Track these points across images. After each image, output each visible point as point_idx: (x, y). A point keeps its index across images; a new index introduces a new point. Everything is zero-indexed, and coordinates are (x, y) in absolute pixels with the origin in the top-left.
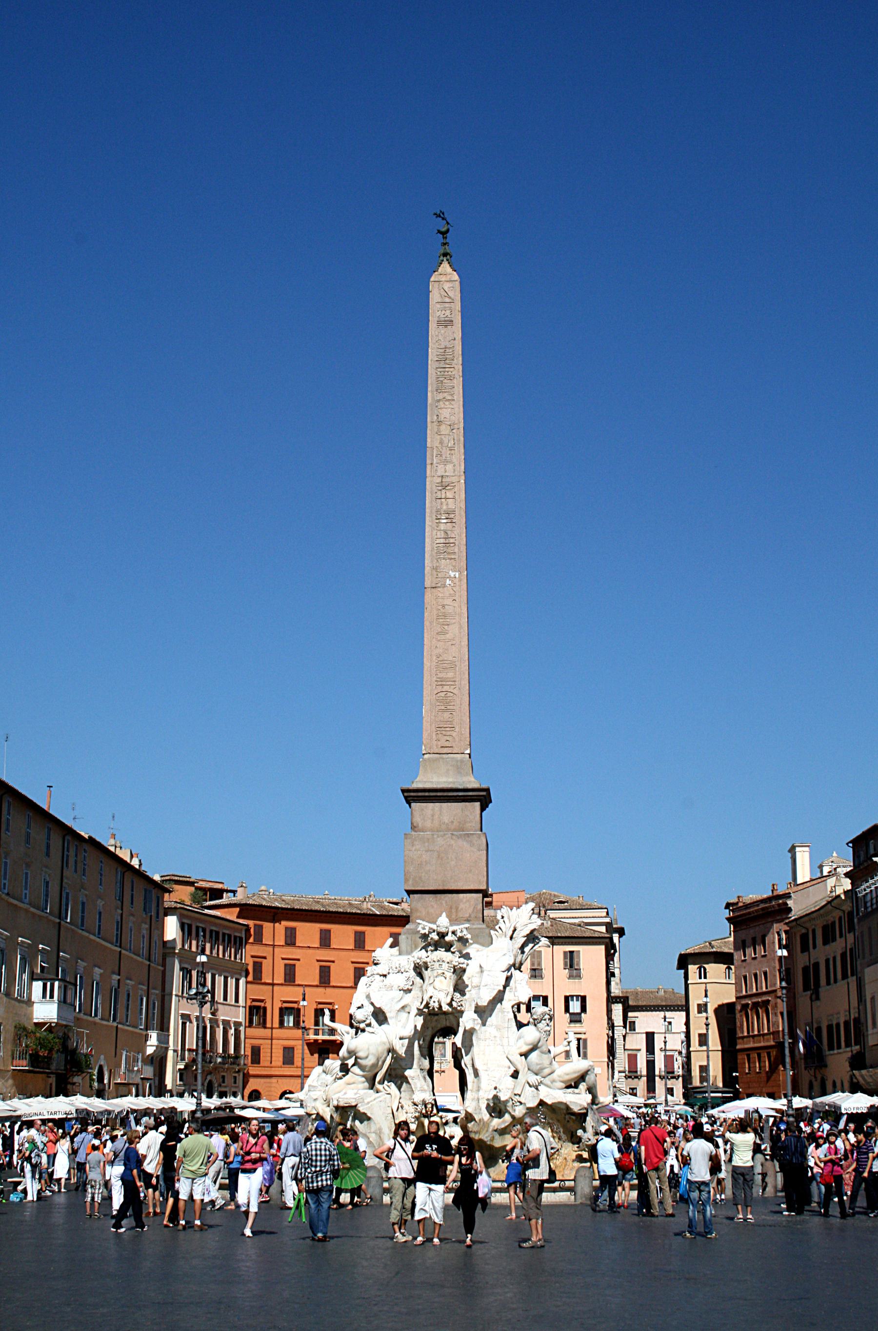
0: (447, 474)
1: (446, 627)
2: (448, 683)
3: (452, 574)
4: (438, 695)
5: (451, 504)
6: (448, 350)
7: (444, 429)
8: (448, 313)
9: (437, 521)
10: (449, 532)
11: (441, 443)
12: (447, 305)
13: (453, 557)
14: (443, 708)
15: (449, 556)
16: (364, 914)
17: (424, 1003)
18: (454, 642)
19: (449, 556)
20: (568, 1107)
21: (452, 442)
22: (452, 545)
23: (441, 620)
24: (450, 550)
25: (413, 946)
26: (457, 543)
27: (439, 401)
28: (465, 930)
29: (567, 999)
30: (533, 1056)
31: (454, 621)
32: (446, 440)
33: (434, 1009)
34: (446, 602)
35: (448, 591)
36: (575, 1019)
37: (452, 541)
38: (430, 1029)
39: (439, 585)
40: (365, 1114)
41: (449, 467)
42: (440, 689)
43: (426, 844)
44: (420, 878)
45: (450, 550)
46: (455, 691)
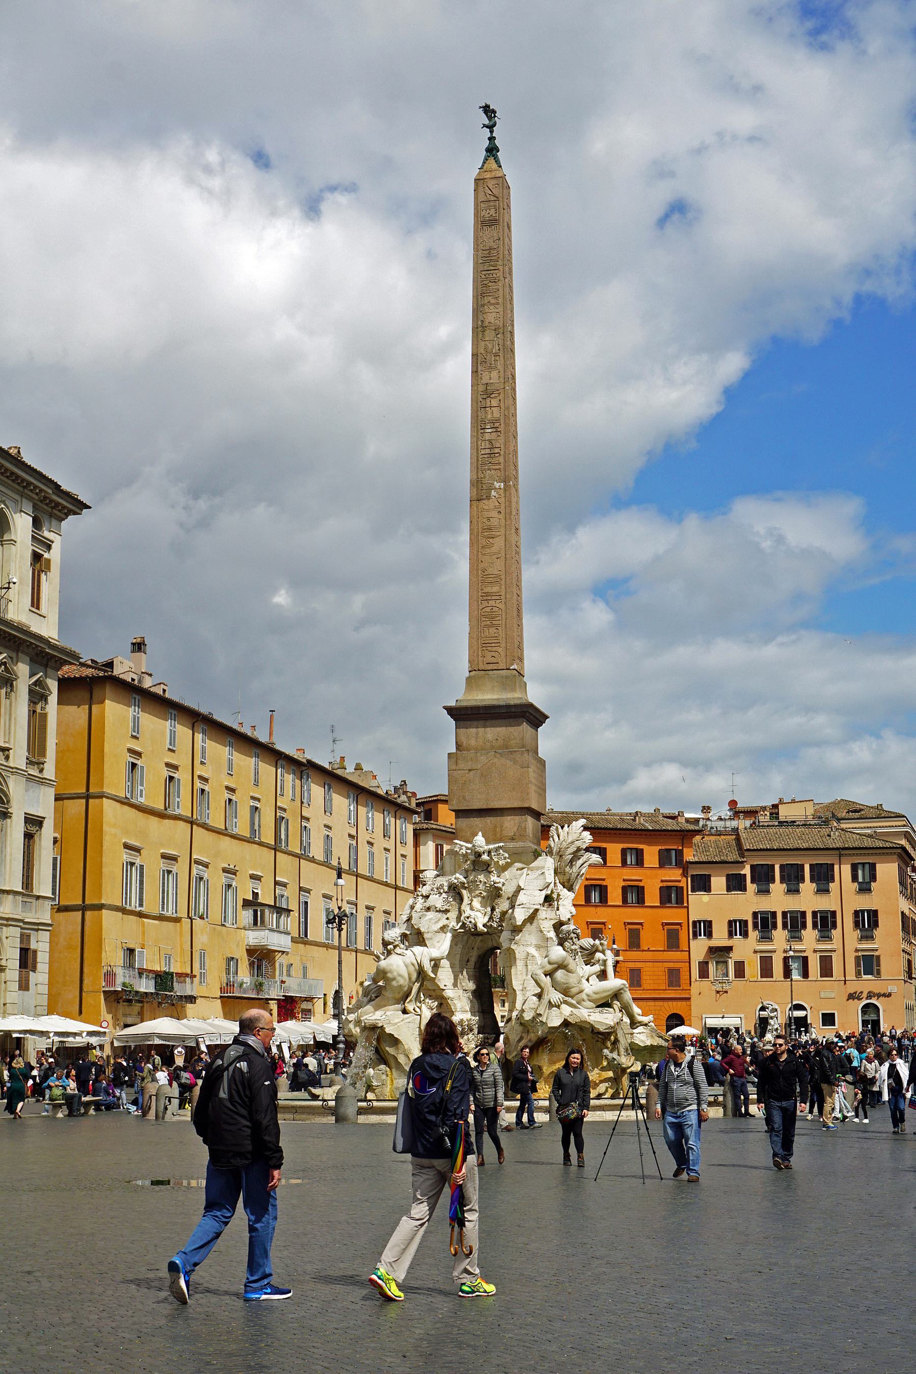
0: (491, 381)
1: (491, 540)
3: (497, 485)
4: (484, 610)
6: (492, 252)
8: (492, 212)
10: (493, 442)
11: (486, 349)
12: (492, 204)
13: (498, 467)
14: (488, 623)
15: (494, 467)
16: (635, 830)
19: (494, 467)
20: (592, 1026)
21: (497, 348)
22: (496, 455)
23: (486, 534)
24: (492, 461)
25: (457, 867)
26: (502, 453)
27: (483, 305)
29: (856, 913)
30: (560, 974)
31: (499, 533)
32: (490, 346)
33: (470, 929)
35: (492, 503)
36: (867, 936)
37: (497, 450)
38: (476, 949)
40: (391, 1035)
41: (494, 374)
42: (485, 604)
43: (470, 763)
44: (464, 797)
45: (494, 460)
46: (502, 606)
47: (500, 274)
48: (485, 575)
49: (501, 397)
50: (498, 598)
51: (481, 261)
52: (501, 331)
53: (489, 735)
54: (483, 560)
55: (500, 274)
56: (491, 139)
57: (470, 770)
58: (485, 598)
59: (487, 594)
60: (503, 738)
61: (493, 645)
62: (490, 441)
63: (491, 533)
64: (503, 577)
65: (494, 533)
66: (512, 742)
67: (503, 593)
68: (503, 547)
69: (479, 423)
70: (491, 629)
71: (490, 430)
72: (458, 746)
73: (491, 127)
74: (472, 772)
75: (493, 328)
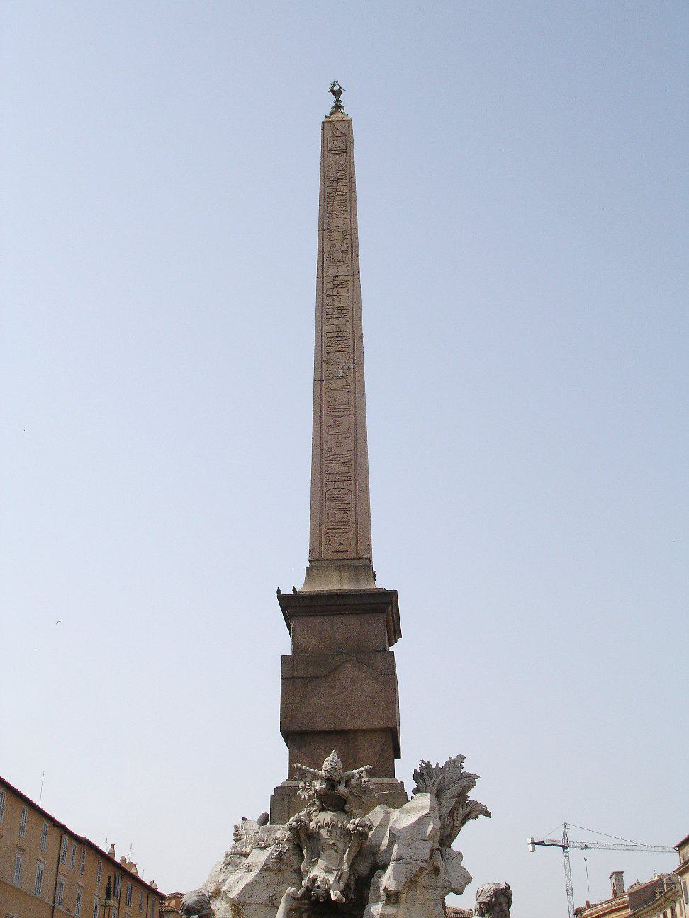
5: (345, 301)
8: (340, 144)
11: (333, 246)
17: (303, 889)
18: (348, 435)
28: (364, 774)
32: (338, 245)
33: (317, 900)
34: (339, 394)
37: (345, 334)
39: (331, 377)
41: (342, 269)
46: (349, 488)
55: (347, 189)
56: (338, 101)
59: (335, 475)
61: (341, 531)
62: (337, 326)
67: (353, 474)
68: (352, 427)
72: (295, 649)
73: (337, 93)
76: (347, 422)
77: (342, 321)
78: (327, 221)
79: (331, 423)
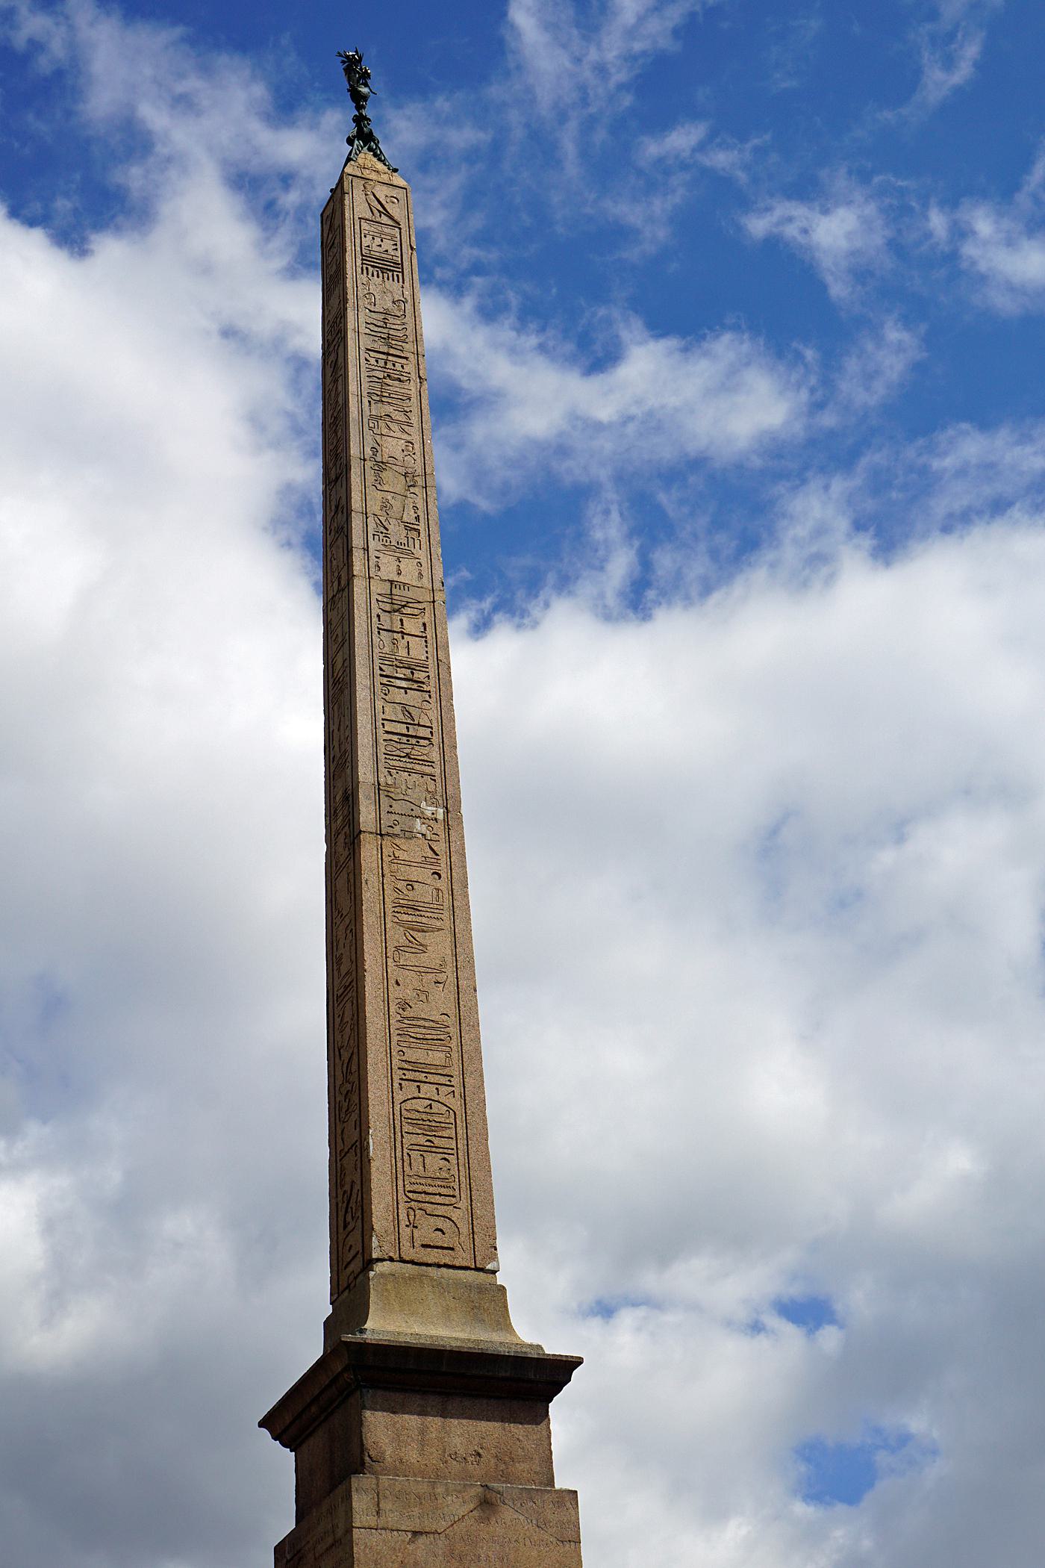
0: (401, 579)
1: (418, 935)
2: (431, 1078)
3: (429, 810)
4: (408, 1105)
5: (418, 650)
6: (391, 320)
7: (393, 481)
9: (385, 680)
11: (386, 506)
14: (422, 1140)
15: (418, 767)
18: (441, 977)
19: (418, 767)
23: (405, 917)
26: (435, 740)
31: (438, 924)
32: (397, 504)
34: (415, 874)
37: (423, 732)
39: (397, 830)
41: (408, 566)
42: (411, 1089)
47: (410, 368)
48: (407, 1018)
49: (427, 618)
50: (443, 1080)
51: (368, 331)
52: (420, 481)
53: (457, 1441)
54: (400, 980)
55: (410, 368)
57: (415, 1533)
58: (410, 1075)
59: (415, 1066)
60: (493, 1451)
63: (419, 919)
64: (453, 1031)
65: (424, 920)
66: (520, 1466)
67: (455, 1071)
68: (449, 959)
69: (377, 662)
70: (429, 1157)
71: (404, 684)
74: (422, 1540)
75: (402, 470)
76: (438, 945)
77: (413, 698)
78: (369, 442)
79: (403, 941)
